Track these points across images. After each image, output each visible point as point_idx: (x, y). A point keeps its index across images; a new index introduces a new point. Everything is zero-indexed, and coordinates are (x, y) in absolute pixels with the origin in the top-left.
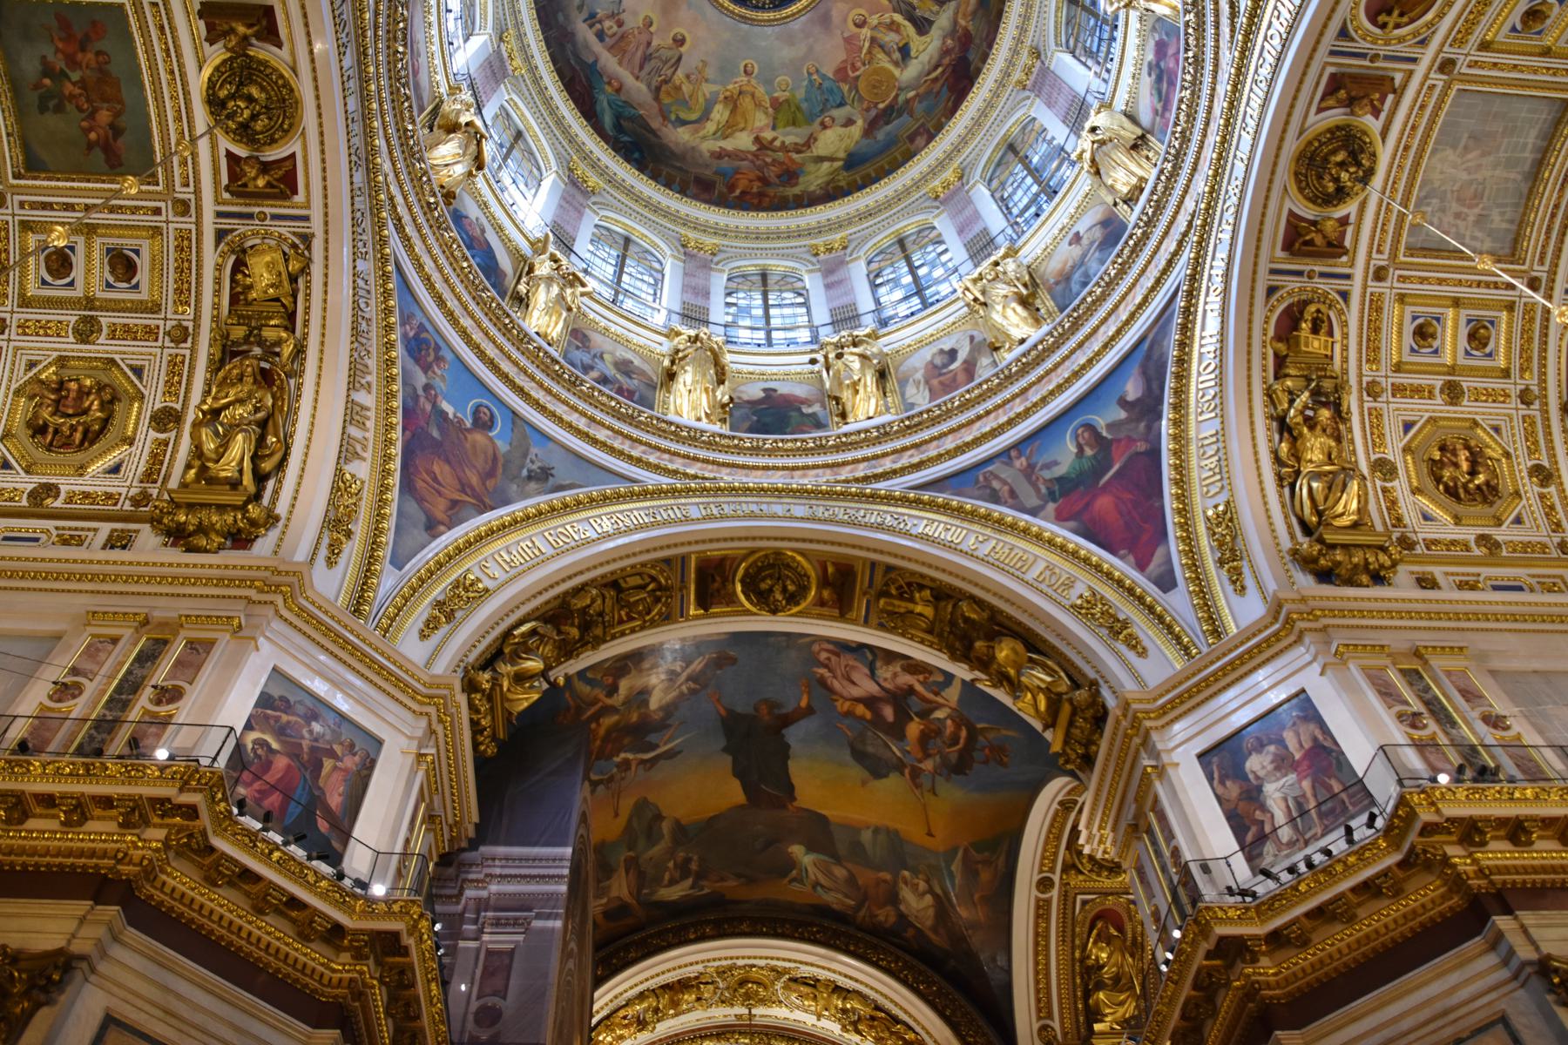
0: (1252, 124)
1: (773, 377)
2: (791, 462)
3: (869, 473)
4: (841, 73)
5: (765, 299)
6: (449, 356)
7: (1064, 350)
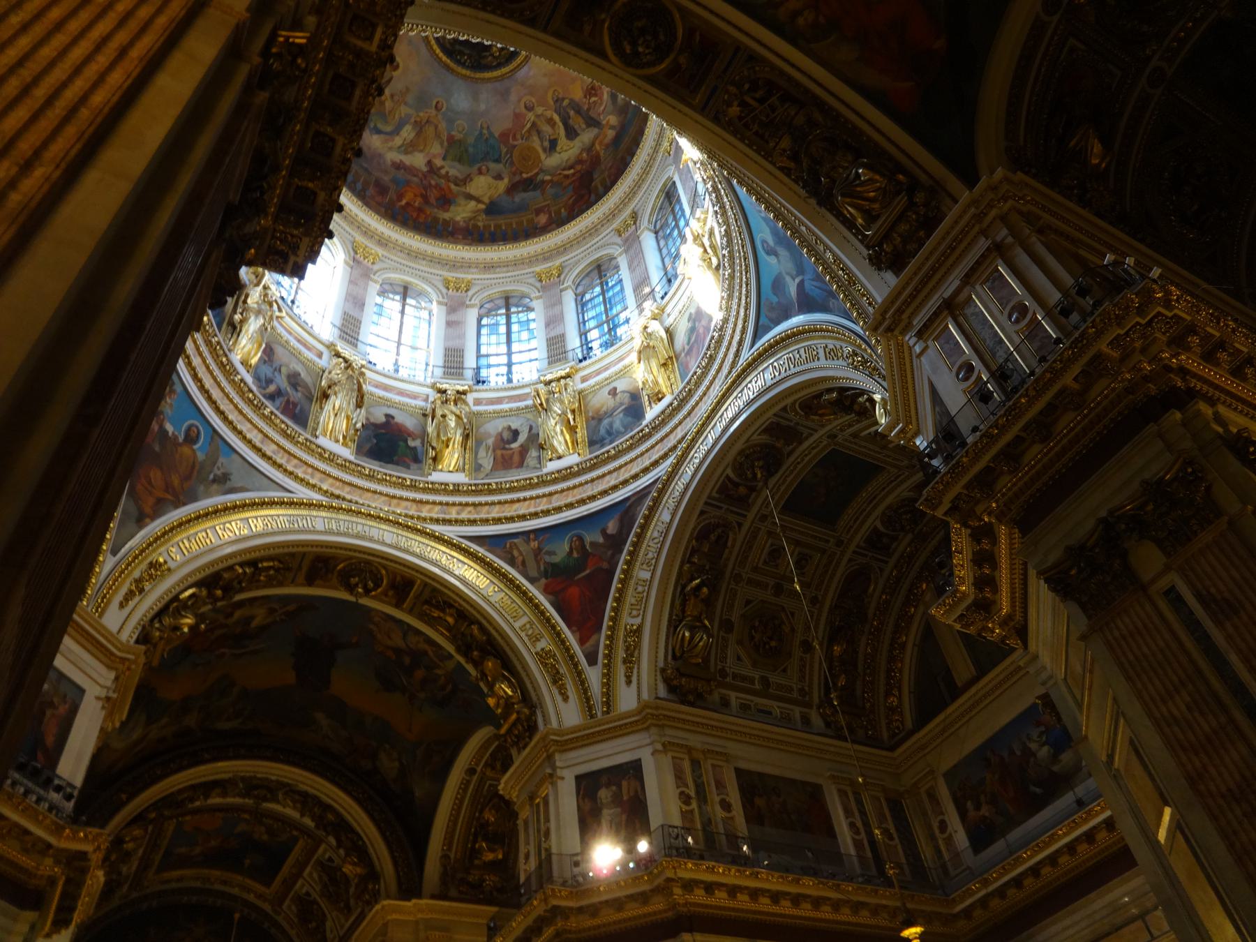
2: (392, 491)
4: (505, 136)
6: (178, 388)
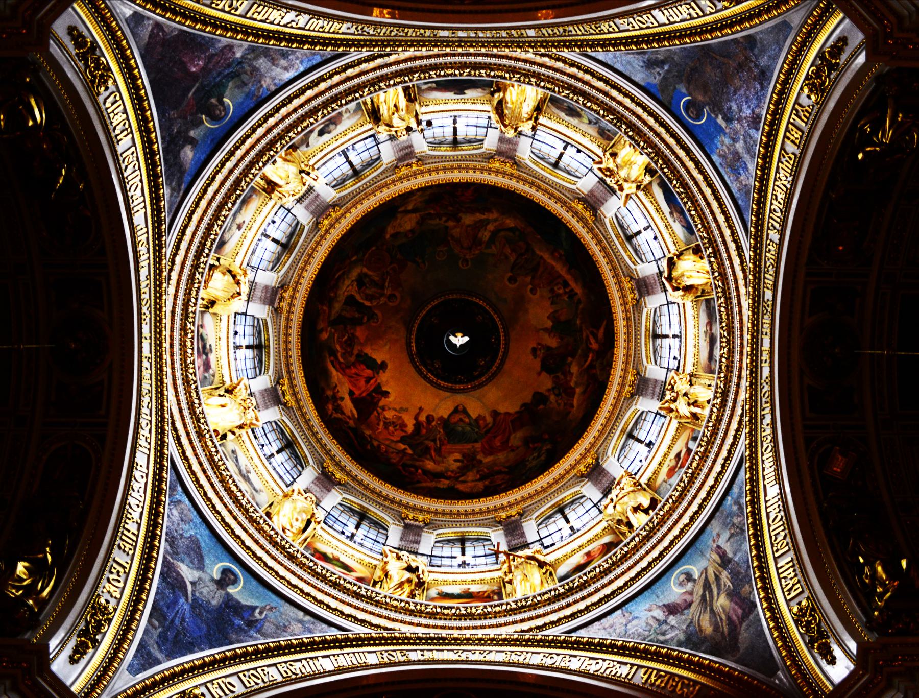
0: (146, 364)
1: (456, 102)
3: (386, 59)
5: (455, 129)
7: (242, 166)
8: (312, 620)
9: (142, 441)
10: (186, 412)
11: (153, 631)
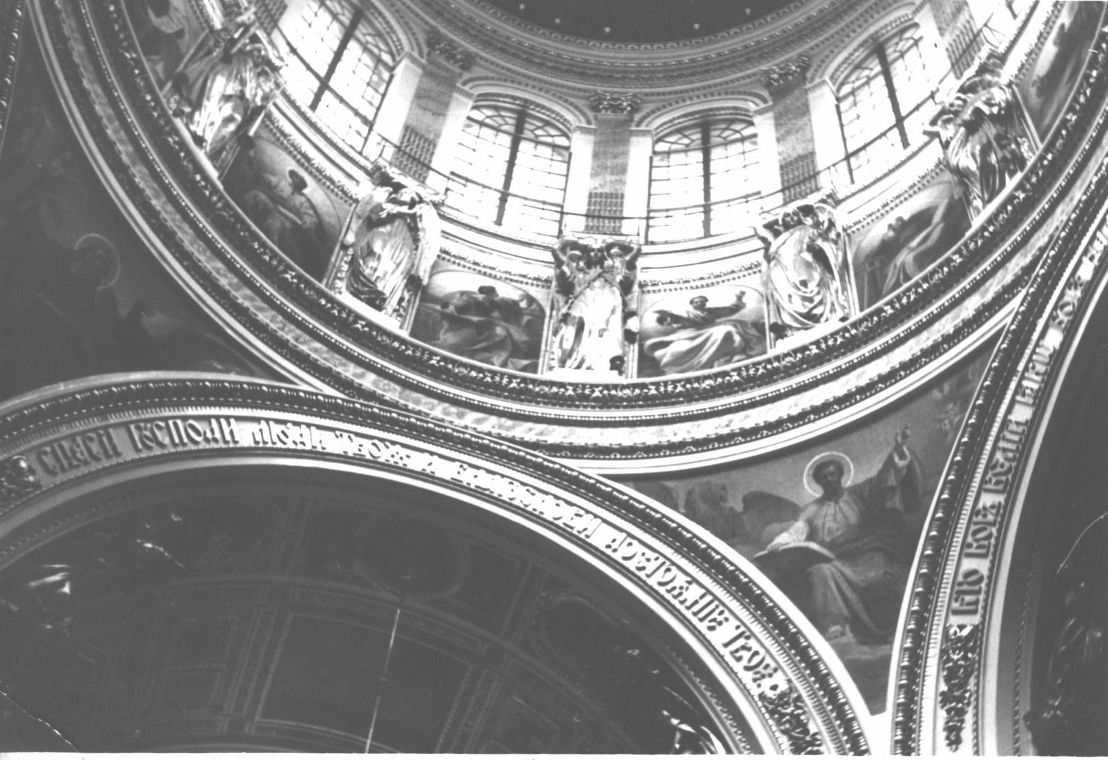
0: (467, 477)
8: (955, 379)
9: (578, 525)
10: (565, 413)
11: (844, 640)
